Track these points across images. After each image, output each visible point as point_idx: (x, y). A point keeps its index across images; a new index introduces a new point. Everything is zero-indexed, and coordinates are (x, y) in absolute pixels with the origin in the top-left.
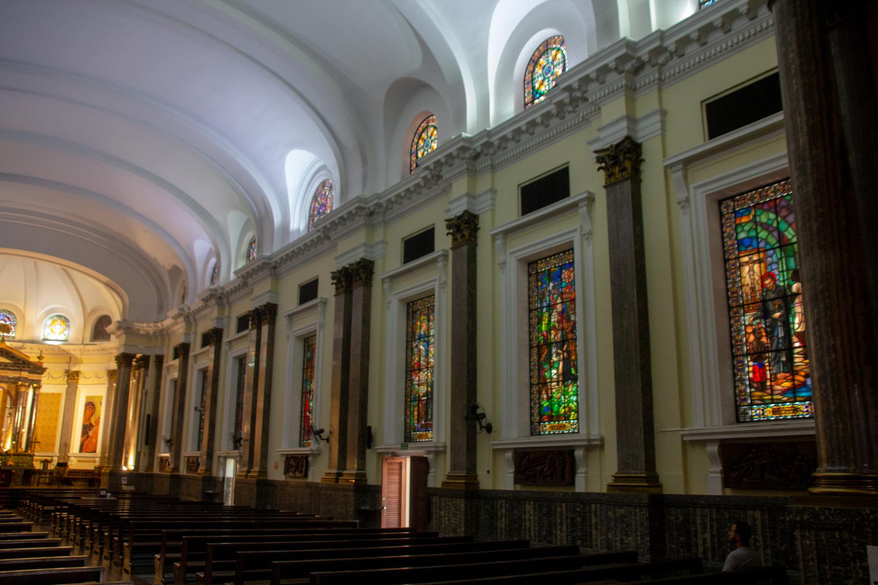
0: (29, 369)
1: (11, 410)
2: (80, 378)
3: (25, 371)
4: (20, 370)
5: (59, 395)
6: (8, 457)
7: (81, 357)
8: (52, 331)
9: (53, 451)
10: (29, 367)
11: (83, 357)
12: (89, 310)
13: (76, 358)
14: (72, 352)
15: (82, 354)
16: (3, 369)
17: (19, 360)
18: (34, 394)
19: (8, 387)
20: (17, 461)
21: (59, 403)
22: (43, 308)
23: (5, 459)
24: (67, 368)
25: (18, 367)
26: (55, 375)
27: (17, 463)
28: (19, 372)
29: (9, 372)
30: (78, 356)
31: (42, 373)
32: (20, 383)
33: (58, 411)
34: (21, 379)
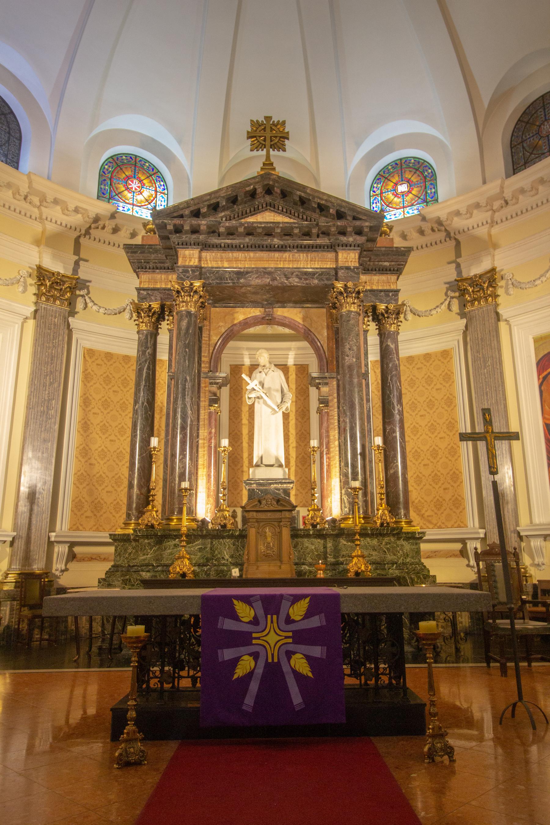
0: (361, 239)
1: (325, 389)
2: (500, 291)
3: (346, 246)
4: (332, 248)
5: (446, 354)
6: (343, 541)
7: (490, 236)
8: (389, 204)
9: (462, 524)
10: (359, 232)
11: (495, 231)
12: (486, 100)
13: (476, 239)
14: (458, 223)
15: (493, 223)
16: (282, 249)
17: (322, 209)
18: (382, 335)
19: (304, 319)
20: (375, 555)
21: (448, 377)
22: (358, 145)
23: (336, 551)
24: (452, 276)
25: (326, 233)
26: (420, 307)
27: (379, 564)
28: (331, 255)
29: (302, 256)
30: (482, 232)
31: (397, 271)
32: (339, 285)
33: (450, 401)
34: (341, 273)
